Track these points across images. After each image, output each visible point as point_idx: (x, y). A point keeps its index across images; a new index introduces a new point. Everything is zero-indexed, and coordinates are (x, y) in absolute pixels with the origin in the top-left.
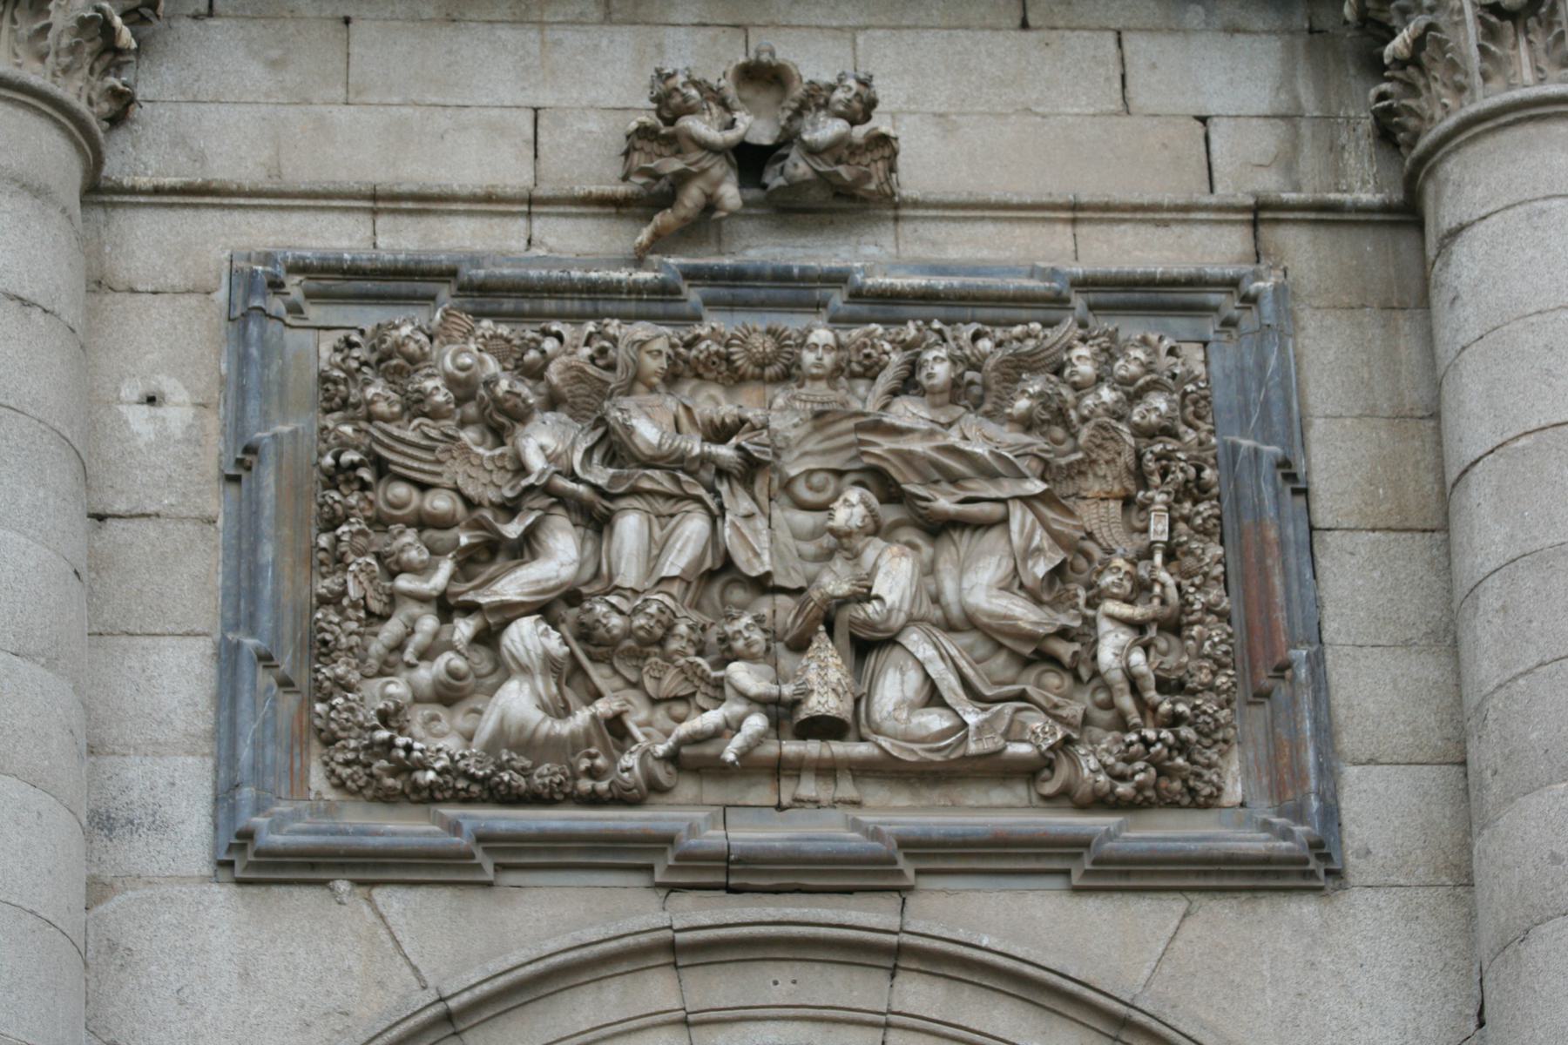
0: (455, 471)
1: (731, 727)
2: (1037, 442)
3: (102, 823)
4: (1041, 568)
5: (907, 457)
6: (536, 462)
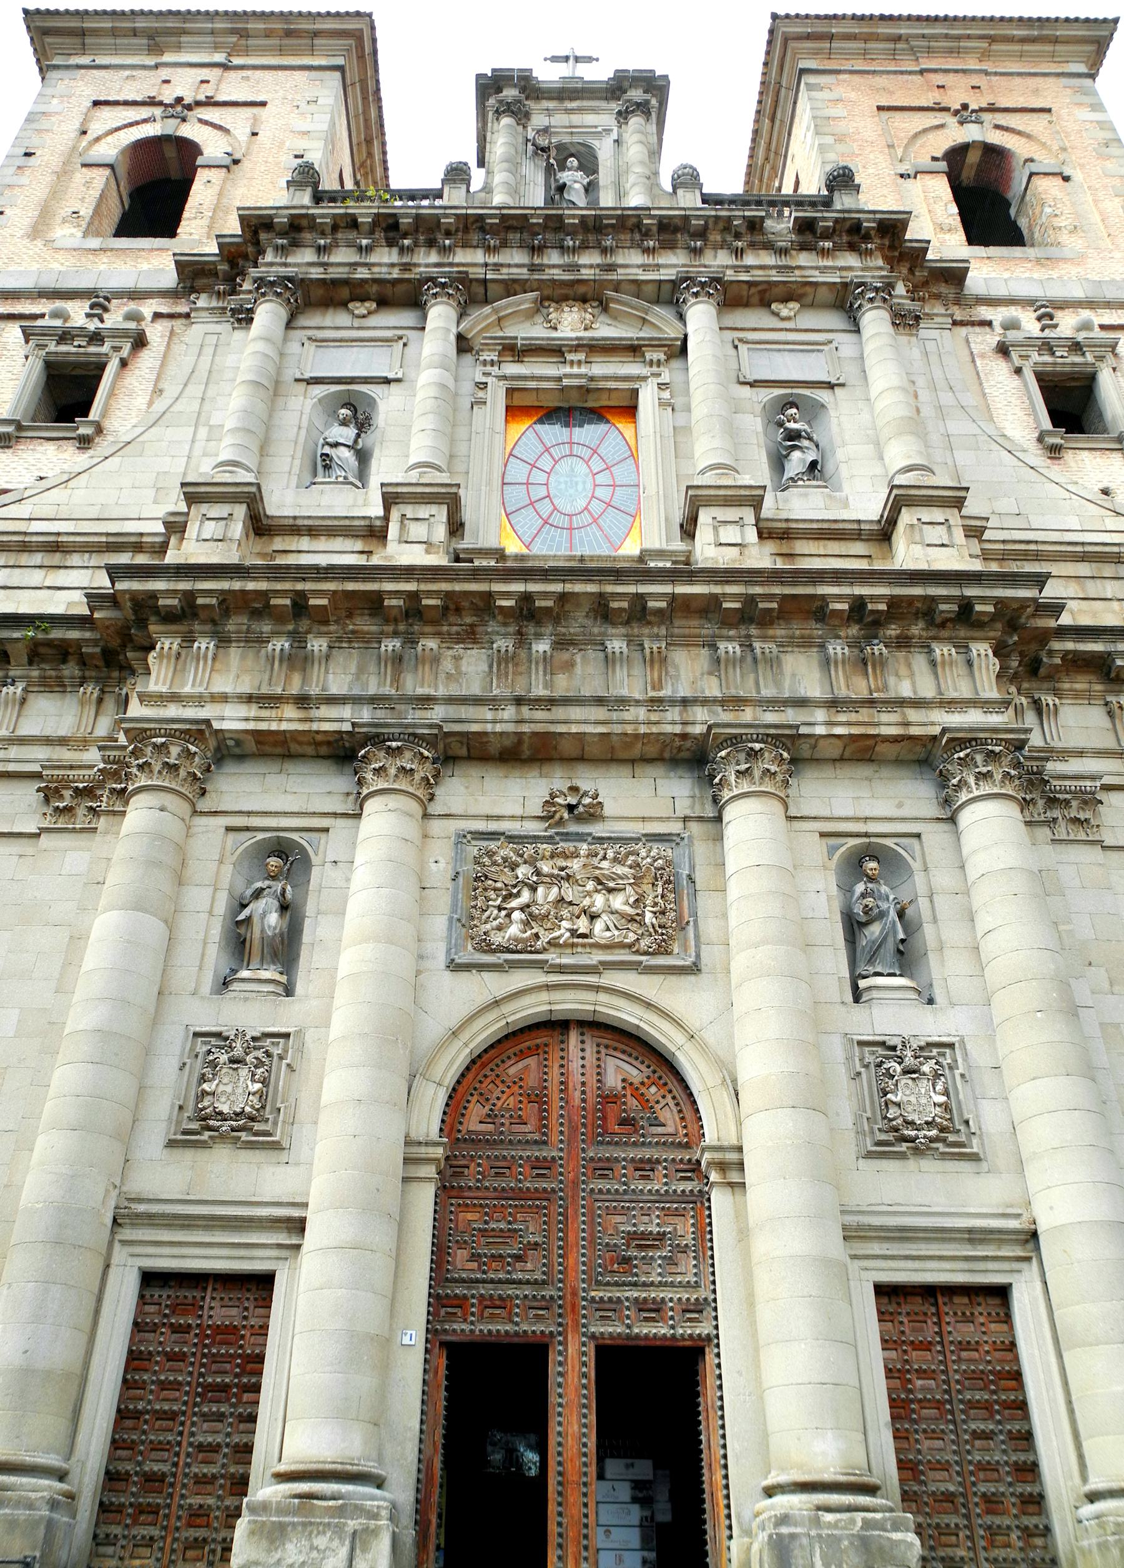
0: (503, 878)
1: (562, 935)
2: (632, 871)
3: (421, 957)
4: (632, 900)
5: (603, 875)
6: (520, 876)
